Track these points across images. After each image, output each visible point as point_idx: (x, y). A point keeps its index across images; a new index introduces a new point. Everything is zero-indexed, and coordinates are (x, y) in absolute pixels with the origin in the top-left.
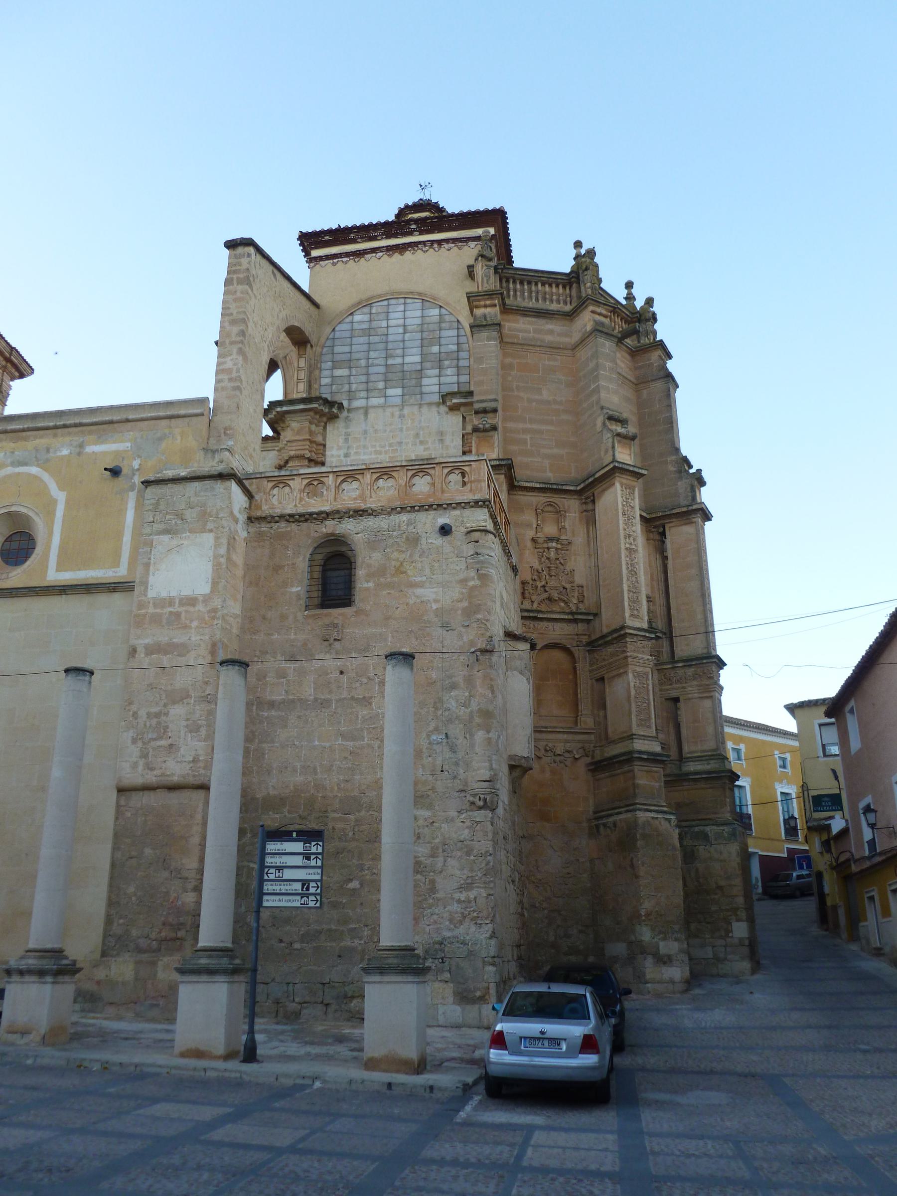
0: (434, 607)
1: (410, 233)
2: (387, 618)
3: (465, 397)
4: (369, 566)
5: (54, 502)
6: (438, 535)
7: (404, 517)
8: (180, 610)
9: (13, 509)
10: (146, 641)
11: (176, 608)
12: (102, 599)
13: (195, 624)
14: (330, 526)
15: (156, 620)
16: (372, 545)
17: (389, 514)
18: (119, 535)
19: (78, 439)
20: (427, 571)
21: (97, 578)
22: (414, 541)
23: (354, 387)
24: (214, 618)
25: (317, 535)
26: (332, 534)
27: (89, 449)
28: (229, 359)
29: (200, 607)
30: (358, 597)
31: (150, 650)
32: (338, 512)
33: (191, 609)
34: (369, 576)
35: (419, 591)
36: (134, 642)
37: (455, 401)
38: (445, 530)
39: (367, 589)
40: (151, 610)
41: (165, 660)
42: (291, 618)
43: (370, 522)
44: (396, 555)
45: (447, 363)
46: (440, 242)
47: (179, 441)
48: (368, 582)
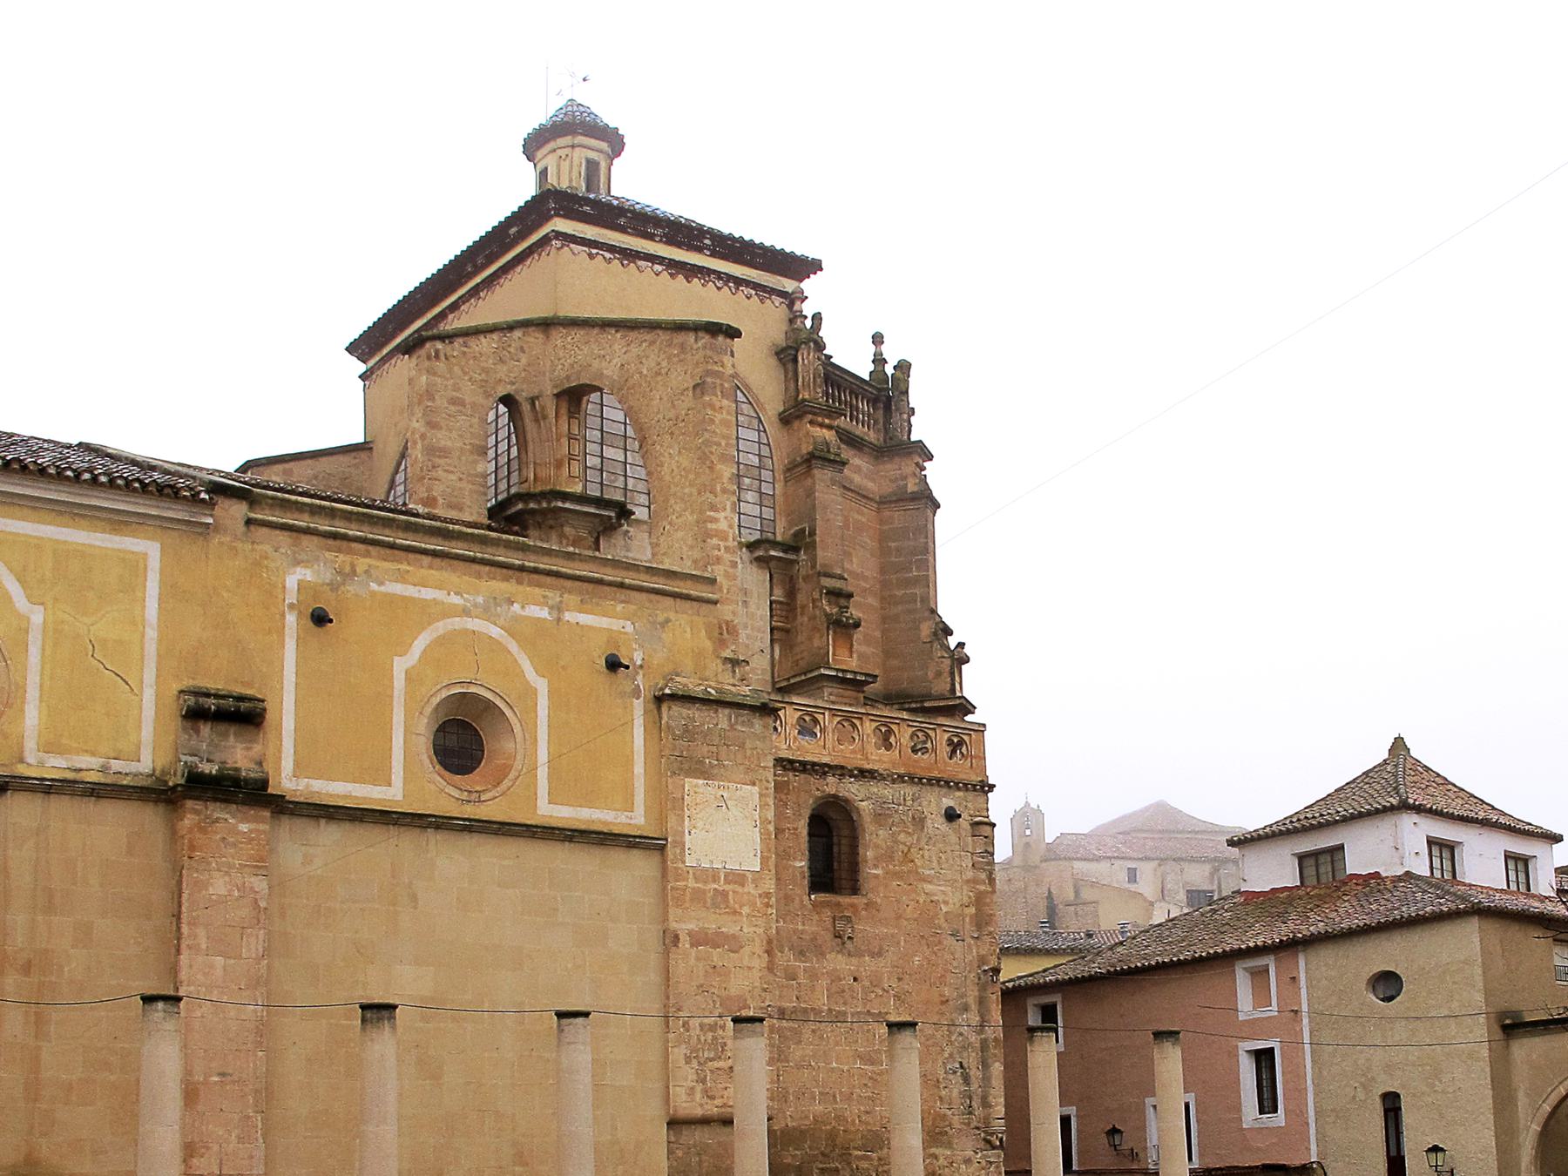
0: (945, 909)
1: (699, 250)
2: (899, 917)
3: (785, 551)
4: (877, 846)
5: (534, 692)
6: (943, 820)
7: (908, 790)
8: (727, 887)
9: (472, 689)
10: (691, 926)
11: (721, 885)
12: (617, 855)
13: (746, 910)
14: (831, 785)
15: (698, 896)
16: (880, 817)
17: (894, 781)
18: (629, 762)
19: (554, 597)
20: (935, 864)
21: (605, 823)
22: (919, 822)
23: (631, 482)
24: (768, 905)
25: (818, 794)
26: (834, 796)
27: (568, 616)
28: (721, 515)
29: (750, 888)
30: (866, 885)
31: (698, 939)
32: (842, 767)
33: (740, 889)
34: (878, 860)
35: (929, 887)
36: (674, 925)
37: (773, 553)
38: (951, 816)
39: (876, 876)
40: (691, 883)
41: (716, 955)
42: (797, 901)
43: (875, 788)
44: (902, 837)
45: (747, 481)
46: (739, 282)
47: (688, 635)
48: (876, 867)
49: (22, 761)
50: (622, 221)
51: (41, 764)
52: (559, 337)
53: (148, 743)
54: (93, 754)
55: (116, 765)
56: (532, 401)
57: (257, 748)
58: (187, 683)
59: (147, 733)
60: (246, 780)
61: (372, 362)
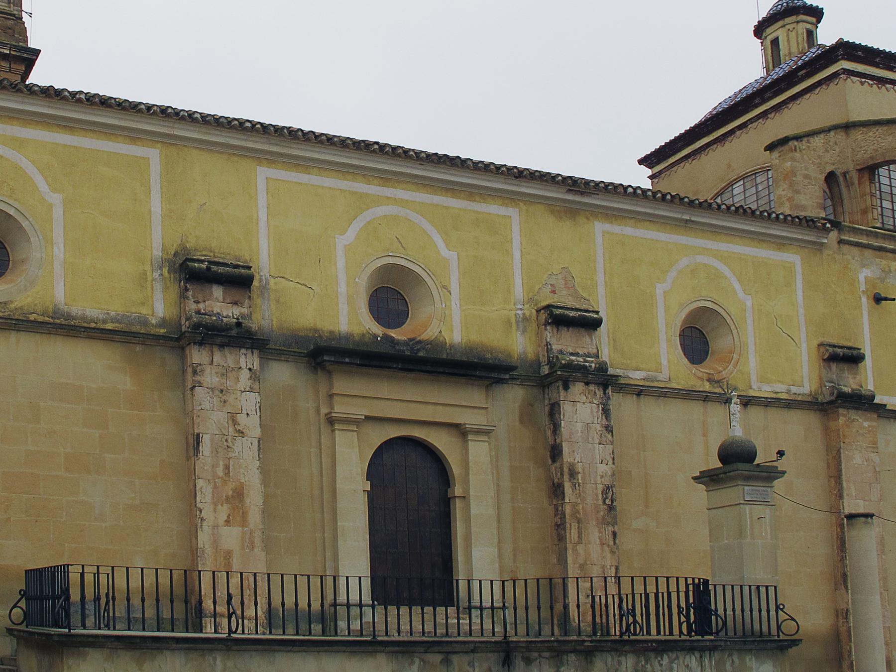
49: (751, 388)
50: (878, 60)
51: (760, 389)
52: (858, 134)
53: (805, 376)
54: (782, 383)
55: (794, 389)
56: (844, 174)
57: (858, 377)
58: (821, 339)
59: (805, 370)
60: (864, 396)
61: (658, 169)
